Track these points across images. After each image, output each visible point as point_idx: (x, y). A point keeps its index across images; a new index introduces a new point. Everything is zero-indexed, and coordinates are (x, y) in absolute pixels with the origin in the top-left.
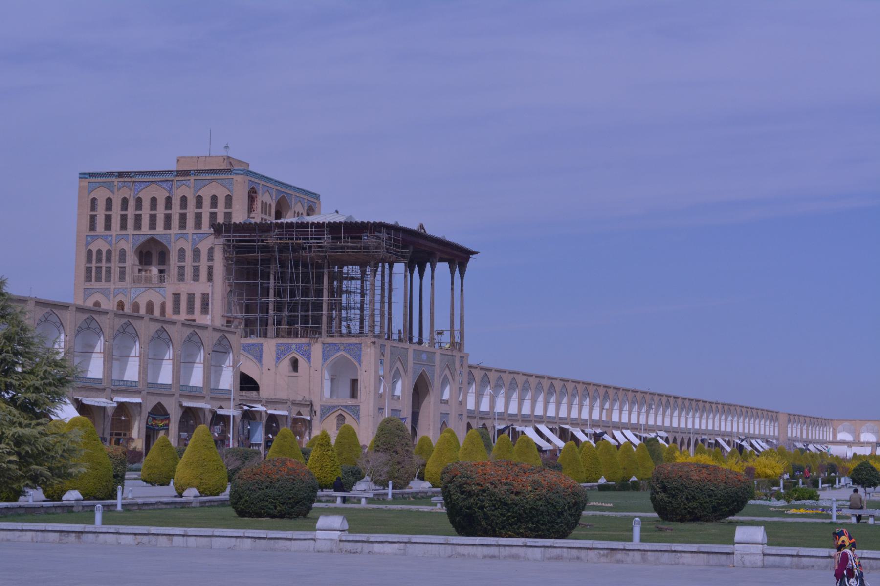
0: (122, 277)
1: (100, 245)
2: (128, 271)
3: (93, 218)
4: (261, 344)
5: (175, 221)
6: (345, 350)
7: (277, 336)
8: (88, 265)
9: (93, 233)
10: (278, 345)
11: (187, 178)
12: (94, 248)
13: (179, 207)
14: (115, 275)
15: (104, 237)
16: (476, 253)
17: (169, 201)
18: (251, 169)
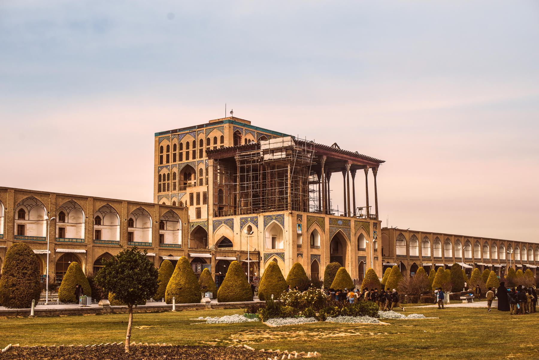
0: (175, 189)
1: (165, 171)
2: (177, 184)
3: (161, 157)
4: (233, 219)
5: (198, 155)
6: (276, 219)
7: (241, 214)
8: (160, 183)
9: (161, 165)
10: (241, 219)
11: (202, 129)
12: (162, 173)
13: (199, 146)
14: (171, 188)
15: (167, 167)
16: (384, 162)
17: (194, 142)
18: (252, 124)
